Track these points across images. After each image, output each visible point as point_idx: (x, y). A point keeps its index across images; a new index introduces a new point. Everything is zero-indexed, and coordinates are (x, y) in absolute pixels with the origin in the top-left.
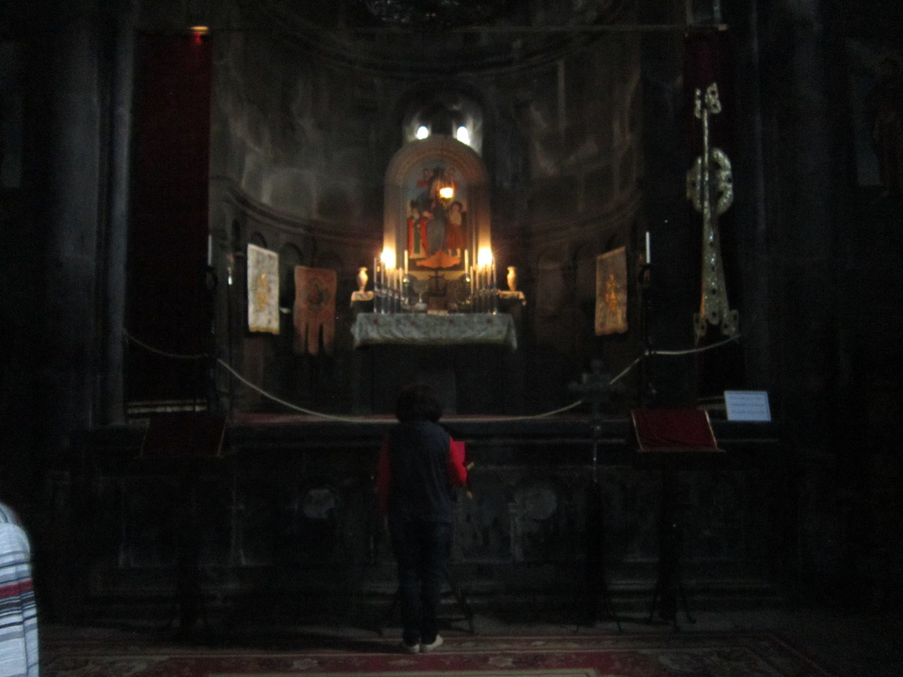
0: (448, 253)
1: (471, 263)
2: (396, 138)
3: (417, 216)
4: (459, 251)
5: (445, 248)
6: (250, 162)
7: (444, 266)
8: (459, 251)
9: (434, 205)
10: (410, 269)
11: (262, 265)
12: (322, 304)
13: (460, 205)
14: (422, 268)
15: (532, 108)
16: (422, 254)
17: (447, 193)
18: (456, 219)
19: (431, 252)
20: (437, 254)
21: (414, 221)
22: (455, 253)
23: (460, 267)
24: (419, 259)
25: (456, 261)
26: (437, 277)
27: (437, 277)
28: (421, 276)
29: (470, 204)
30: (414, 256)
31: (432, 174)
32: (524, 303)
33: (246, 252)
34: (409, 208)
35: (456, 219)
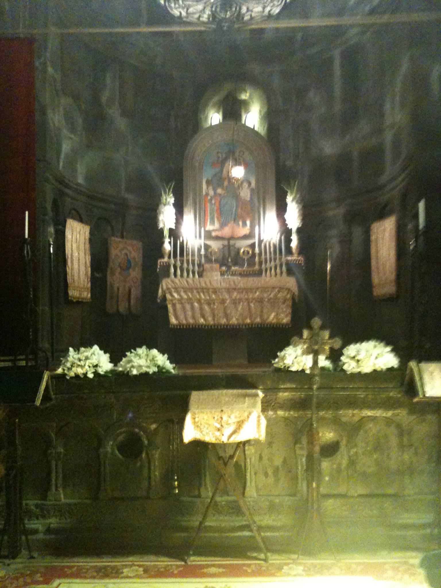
0: (239, 225)
2: (194, 124)
4: (248, 223)
6: (66, 147)
8: (248, 223)
9: (226, 183)
11: (77, 236)
12: (131, 270)
13: (250, 184)
14: (217, 238)
15: (311, 94)
16: (217, 225)
17: (238, 172)
18: (245, 193)
19: (222, 225)
20: (229, 225)
21: (209, 198)
22: (244, 224)
23: (250, 236)
24: (213, 230)
25: (246, 231)
26: (229, 246)
27: (229, 246)
28: (215, 245)
30: (209, 227)
31: (224, 156)
33: (64, 226)
34: (204, 186)
35: (245, 193)
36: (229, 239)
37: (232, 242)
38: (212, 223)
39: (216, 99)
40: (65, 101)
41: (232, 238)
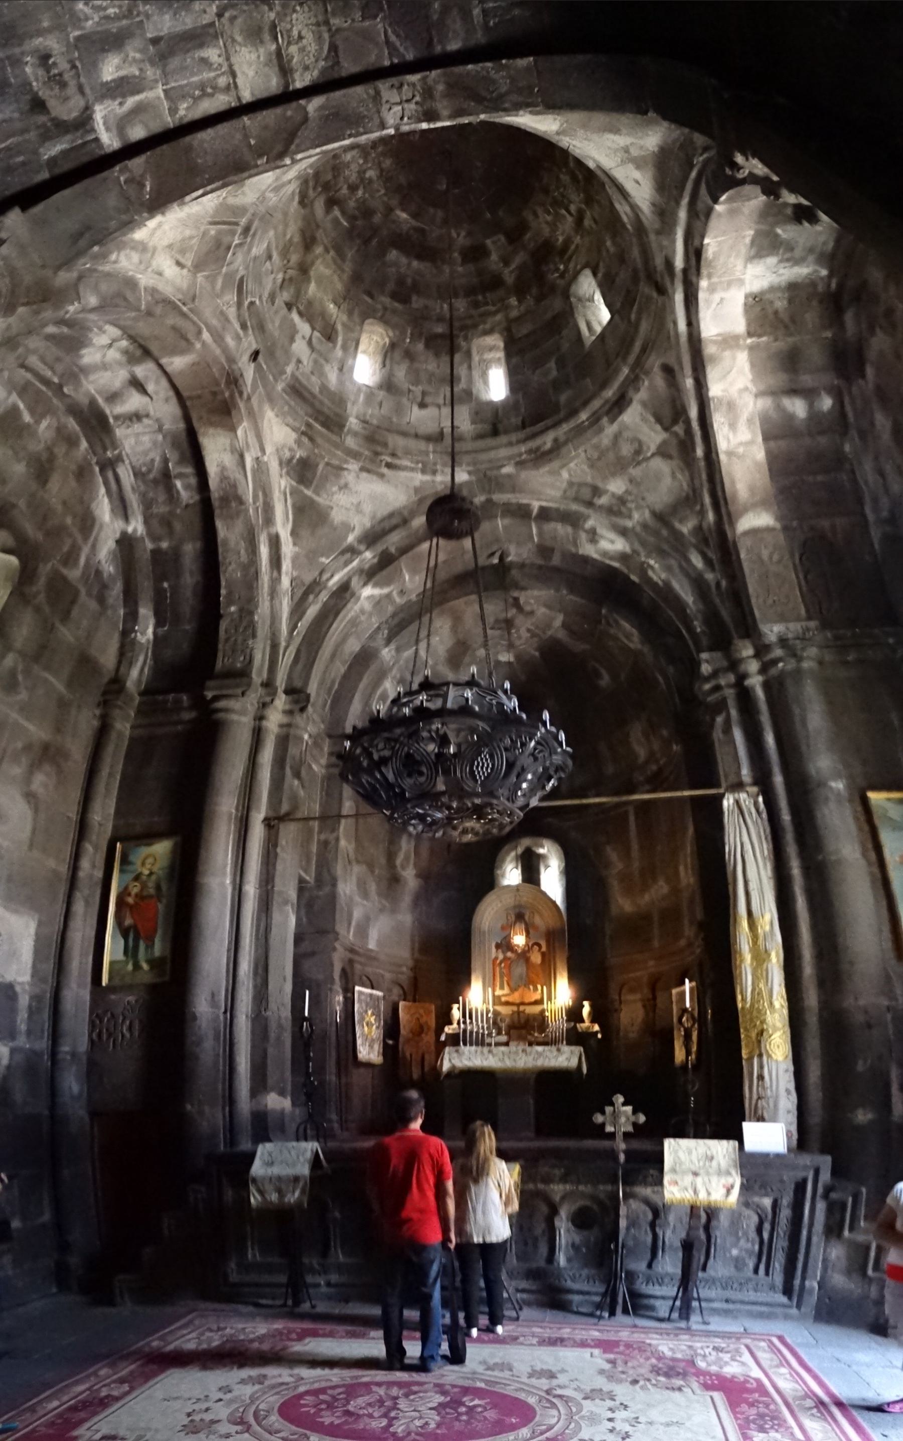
1: (549, 999)
3: (501, 957)
5: (526, 985)
7: (526, 1001)
8: (539, 987)
10: (494, 1004)
13: (539, 946)
14: (507, 1003)
16: (506, 990)
19: (513, 990)
20: (520, 990)
22: (536, 989)
25: (537, 996)
26: (519, 1012)
27: (519, 1012)
28: (504, 1010)
29: (548, 946)
30: (498, 992)
32: (599, 1036)
34: (494, 950)
36: (518, 1005)
37: (522, 1008)
38: (502, 988)
39: (513, 854)
40: (357, 869)
41: (523, 1004)
